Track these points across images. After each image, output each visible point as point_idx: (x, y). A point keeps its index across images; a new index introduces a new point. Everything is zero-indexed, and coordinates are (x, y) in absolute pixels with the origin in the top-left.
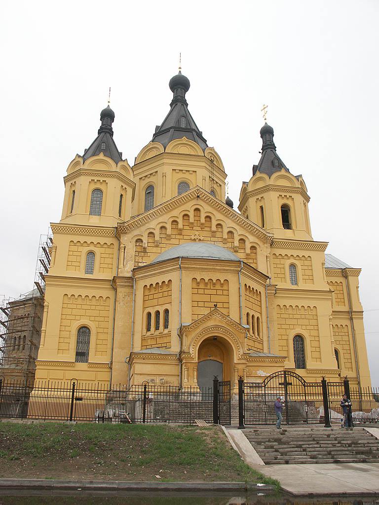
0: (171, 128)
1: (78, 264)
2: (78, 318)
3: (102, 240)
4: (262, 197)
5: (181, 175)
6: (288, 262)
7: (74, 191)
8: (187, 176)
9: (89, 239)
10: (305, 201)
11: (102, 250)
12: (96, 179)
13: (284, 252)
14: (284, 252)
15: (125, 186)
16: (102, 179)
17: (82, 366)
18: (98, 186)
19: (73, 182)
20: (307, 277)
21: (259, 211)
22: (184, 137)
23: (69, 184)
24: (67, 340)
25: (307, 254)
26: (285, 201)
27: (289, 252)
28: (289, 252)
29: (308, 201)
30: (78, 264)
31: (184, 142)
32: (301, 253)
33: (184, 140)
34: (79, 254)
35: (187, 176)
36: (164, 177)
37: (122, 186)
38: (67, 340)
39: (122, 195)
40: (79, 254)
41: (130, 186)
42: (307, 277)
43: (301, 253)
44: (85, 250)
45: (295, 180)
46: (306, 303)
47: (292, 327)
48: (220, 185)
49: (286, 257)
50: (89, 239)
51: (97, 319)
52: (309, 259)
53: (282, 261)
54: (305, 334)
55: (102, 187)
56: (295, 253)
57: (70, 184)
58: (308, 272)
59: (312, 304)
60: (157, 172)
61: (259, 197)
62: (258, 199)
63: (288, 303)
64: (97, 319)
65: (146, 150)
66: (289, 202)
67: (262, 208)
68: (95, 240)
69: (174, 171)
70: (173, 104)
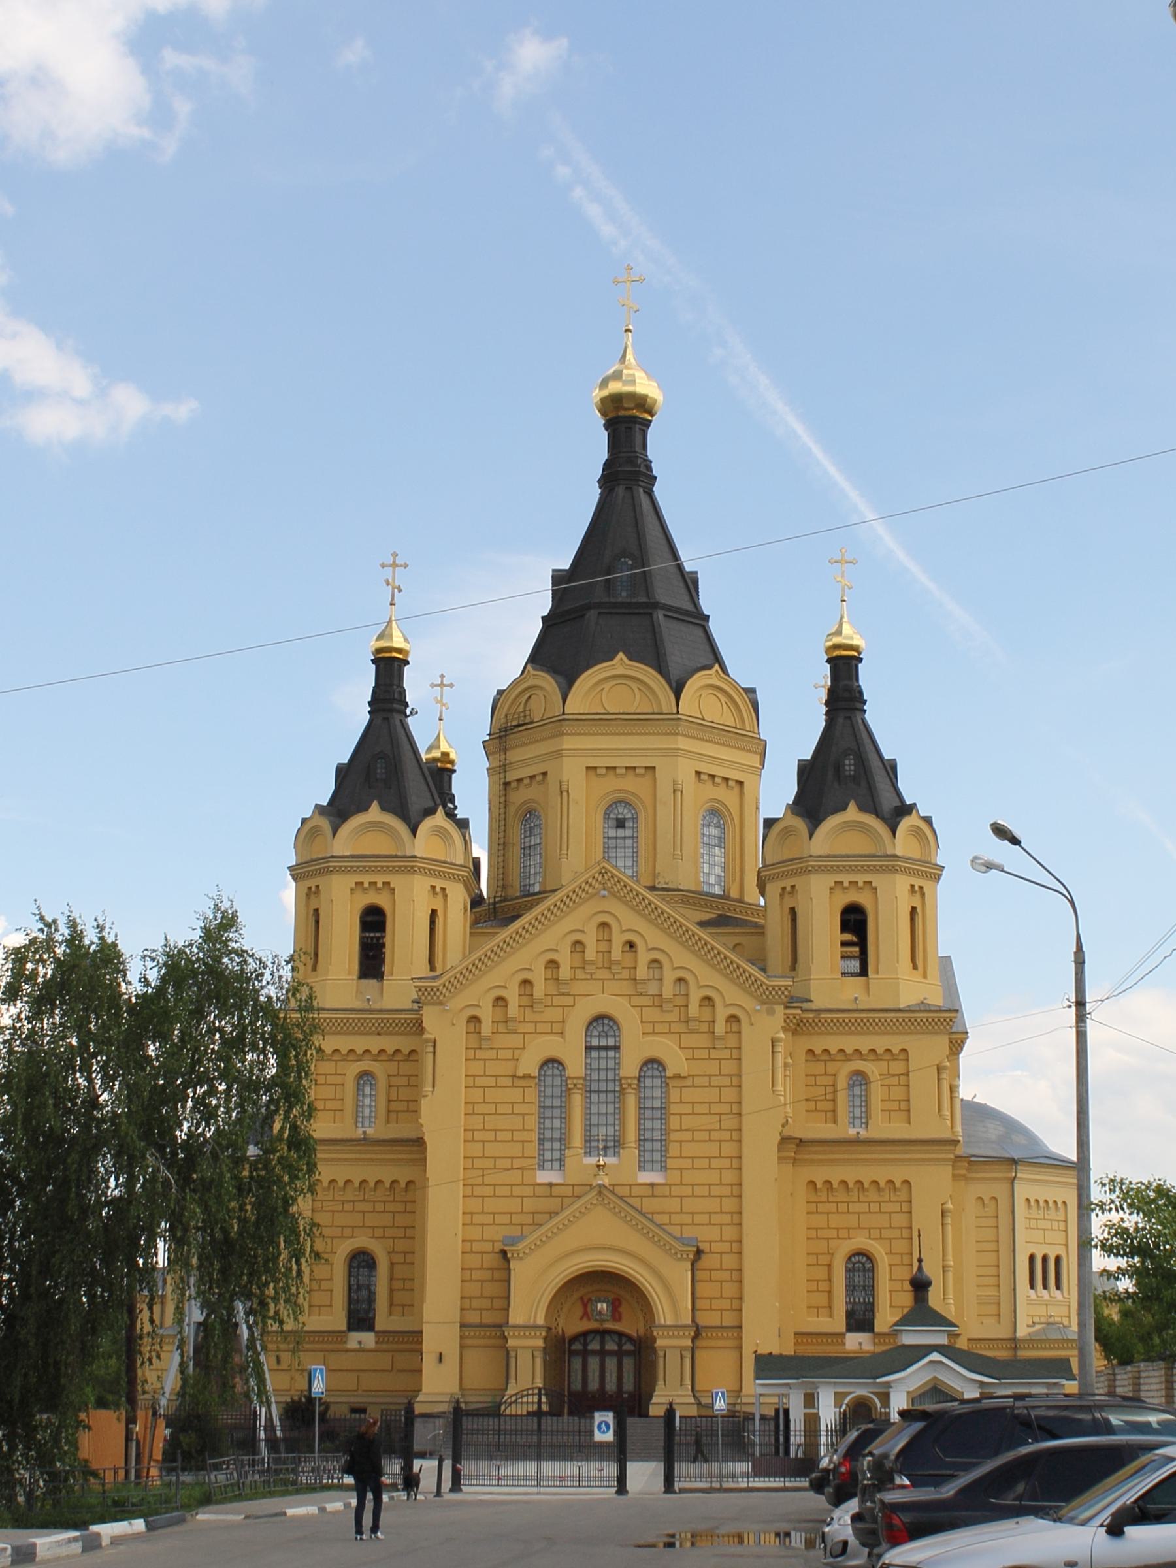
0: (588, 607)
1: (336, 1105)
2: (348, 1232)
3: (389, 1043)
4: (793, 887)
5: (611, 784)
6: (845, 1070)
7: (316, 911)
8: (630, 784)
9: (360, 1043)
10: (918, 882)
11: (392, 1067)
12: (366, 879)
13: (833, 1043)
14: (833, 1043)
15: (439, 884)
16: (380, 880)
17: (357, 1339)
19: (312, 883)
20: (895, 1106)
21: (787, 918)
22: (621, 655)
24: (325, 1286)
25: (895, 1043)
26: (853, 897)
27: (850, 1043)
28: (850, 1043)
29: (937, 878)
30: (336, 1105)
31: (620, 671)
32: (880, 1043)
33: (621, 663)
34: (338, 1080)
35: (630, 784)
36: (565, 794)
37: (433, 887)
38: (325, 1286)
39: (434, 913)
40: (338, 1080)
41: (452, 877)
42: (895, 1106)
43: (880, 1043)
44: (354, 1069)
46: (882, 1174)
47: (843, 1233)
48: (741, 783)
49: (840, 1056)
50: (360, 1043)
51: (389, 1233)
52: (902, 1057)
53: (832, 1067)
54: (878, 1250)
56: (864, 1043)
58: (897, 1093)
59: (898, 1174)
60: (545, 774)
61: (788, 883)
62: (784, 889)
63: (836, 1174)
64: (389, 1233)
66: (864, 899)
67: (793, 912)
68: (375, 1044)
69: (592, 773)
70: (611, 478)
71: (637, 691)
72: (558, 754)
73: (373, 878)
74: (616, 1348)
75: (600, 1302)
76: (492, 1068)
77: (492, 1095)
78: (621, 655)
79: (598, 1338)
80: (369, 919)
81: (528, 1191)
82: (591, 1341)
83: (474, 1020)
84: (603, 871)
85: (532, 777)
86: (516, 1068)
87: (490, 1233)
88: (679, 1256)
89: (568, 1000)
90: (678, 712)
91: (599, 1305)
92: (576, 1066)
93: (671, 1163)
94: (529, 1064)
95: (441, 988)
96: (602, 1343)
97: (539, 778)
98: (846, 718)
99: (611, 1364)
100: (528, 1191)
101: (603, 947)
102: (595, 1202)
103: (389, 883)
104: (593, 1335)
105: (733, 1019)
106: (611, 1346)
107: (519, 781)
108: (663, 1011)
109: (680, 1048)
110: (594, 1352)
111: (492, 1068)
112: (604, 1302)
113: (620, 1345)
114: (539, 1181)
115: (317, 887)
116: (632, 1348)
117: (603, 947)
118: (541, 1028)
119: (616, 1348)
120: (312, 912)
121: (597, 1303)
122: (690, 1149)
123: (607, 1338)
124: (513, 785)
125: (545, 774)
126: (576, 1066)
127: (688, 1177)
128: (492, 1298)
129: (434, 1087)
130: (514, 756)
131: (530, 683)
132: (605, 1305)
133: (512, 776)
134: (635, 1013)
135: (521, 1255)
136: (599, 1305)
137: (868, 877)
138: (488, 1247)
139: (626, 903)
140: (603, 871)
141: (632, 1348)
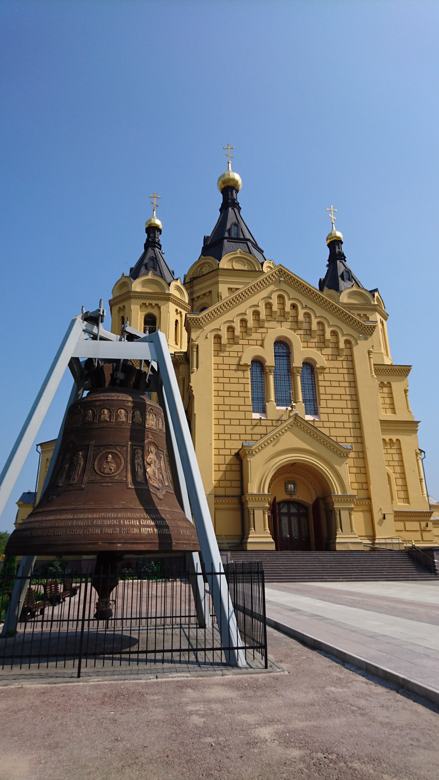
10: (382, 319)
12: (147, 302)
15: (180, 309)
16: (154, 302)
18: (150, 310)
19: (121, 305)
22: (240, 250)
23: (115, 309)
36: (220, 297)
37: (177, 310)
45: (369, 295)
55: (155, 312)
57: (118, 309)
60: (210, 292)
65: (198, 265)
71: (246, 263)
72: (217, 283)
73: (150, 302)
74: (296, 512)
75: (290, 484)
76: (227, 361)
77: (227, 374)
78: (240, 250)
79: (286, 505)
80: (148, 320)
81: (249, 423)
82: (283, 507)
83: (218, 337)
84: (280, 270)
85: (204, 295)
86: (240, 360)
87: (229, 444)
88: (342, 455)
89: (264, 330)
90: (262, 270)
91: (289, 486)
92: (270, 361)
93: (321, 410)
94: (247, 360)
95: (201, 319)
96: (289, 509)
97: (208, 294)
98: (340, 262)
99: (294, 520)
100: (249, 423)
101: (281, 306)
102: (292, 424)
103: (158, 304)
104: (283, 504)
105: (347, 342)
106: (293, 510)
107: (198, 297)
108: (311, 337)
109: (322, 355)
110: (284, 514)
111: (227, 361)
112: (292, 484)
113: (298, 510)
114: (253, 417)
115: (124, 306)
116: (305, 511)
117: (281, 306)
118: (251, 342)
119: (296, 512)
120: (120, 318)
121: (288, 484)
122: (331, 404)
123: (291, 506)
124: (196, 299)
125: (210, 292)
126: (270, 361)
127: (332, 418)
128: (231, 481)
129: (197, 368)
130: (195, 288)
131: (202, 262)
132: (292, 486)
133: (195, 296)
134: (298, 337)
135: (254, 453)
136: (289, 486)
137: (365, 313)
138: (228, 452)
139: (291, 286)
140: (280, 270)
141: (305, 511)
